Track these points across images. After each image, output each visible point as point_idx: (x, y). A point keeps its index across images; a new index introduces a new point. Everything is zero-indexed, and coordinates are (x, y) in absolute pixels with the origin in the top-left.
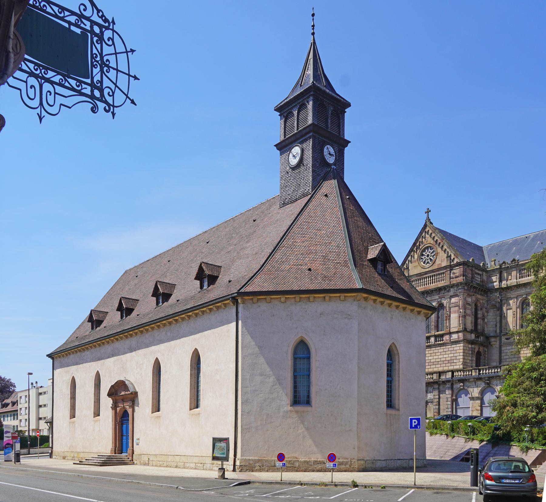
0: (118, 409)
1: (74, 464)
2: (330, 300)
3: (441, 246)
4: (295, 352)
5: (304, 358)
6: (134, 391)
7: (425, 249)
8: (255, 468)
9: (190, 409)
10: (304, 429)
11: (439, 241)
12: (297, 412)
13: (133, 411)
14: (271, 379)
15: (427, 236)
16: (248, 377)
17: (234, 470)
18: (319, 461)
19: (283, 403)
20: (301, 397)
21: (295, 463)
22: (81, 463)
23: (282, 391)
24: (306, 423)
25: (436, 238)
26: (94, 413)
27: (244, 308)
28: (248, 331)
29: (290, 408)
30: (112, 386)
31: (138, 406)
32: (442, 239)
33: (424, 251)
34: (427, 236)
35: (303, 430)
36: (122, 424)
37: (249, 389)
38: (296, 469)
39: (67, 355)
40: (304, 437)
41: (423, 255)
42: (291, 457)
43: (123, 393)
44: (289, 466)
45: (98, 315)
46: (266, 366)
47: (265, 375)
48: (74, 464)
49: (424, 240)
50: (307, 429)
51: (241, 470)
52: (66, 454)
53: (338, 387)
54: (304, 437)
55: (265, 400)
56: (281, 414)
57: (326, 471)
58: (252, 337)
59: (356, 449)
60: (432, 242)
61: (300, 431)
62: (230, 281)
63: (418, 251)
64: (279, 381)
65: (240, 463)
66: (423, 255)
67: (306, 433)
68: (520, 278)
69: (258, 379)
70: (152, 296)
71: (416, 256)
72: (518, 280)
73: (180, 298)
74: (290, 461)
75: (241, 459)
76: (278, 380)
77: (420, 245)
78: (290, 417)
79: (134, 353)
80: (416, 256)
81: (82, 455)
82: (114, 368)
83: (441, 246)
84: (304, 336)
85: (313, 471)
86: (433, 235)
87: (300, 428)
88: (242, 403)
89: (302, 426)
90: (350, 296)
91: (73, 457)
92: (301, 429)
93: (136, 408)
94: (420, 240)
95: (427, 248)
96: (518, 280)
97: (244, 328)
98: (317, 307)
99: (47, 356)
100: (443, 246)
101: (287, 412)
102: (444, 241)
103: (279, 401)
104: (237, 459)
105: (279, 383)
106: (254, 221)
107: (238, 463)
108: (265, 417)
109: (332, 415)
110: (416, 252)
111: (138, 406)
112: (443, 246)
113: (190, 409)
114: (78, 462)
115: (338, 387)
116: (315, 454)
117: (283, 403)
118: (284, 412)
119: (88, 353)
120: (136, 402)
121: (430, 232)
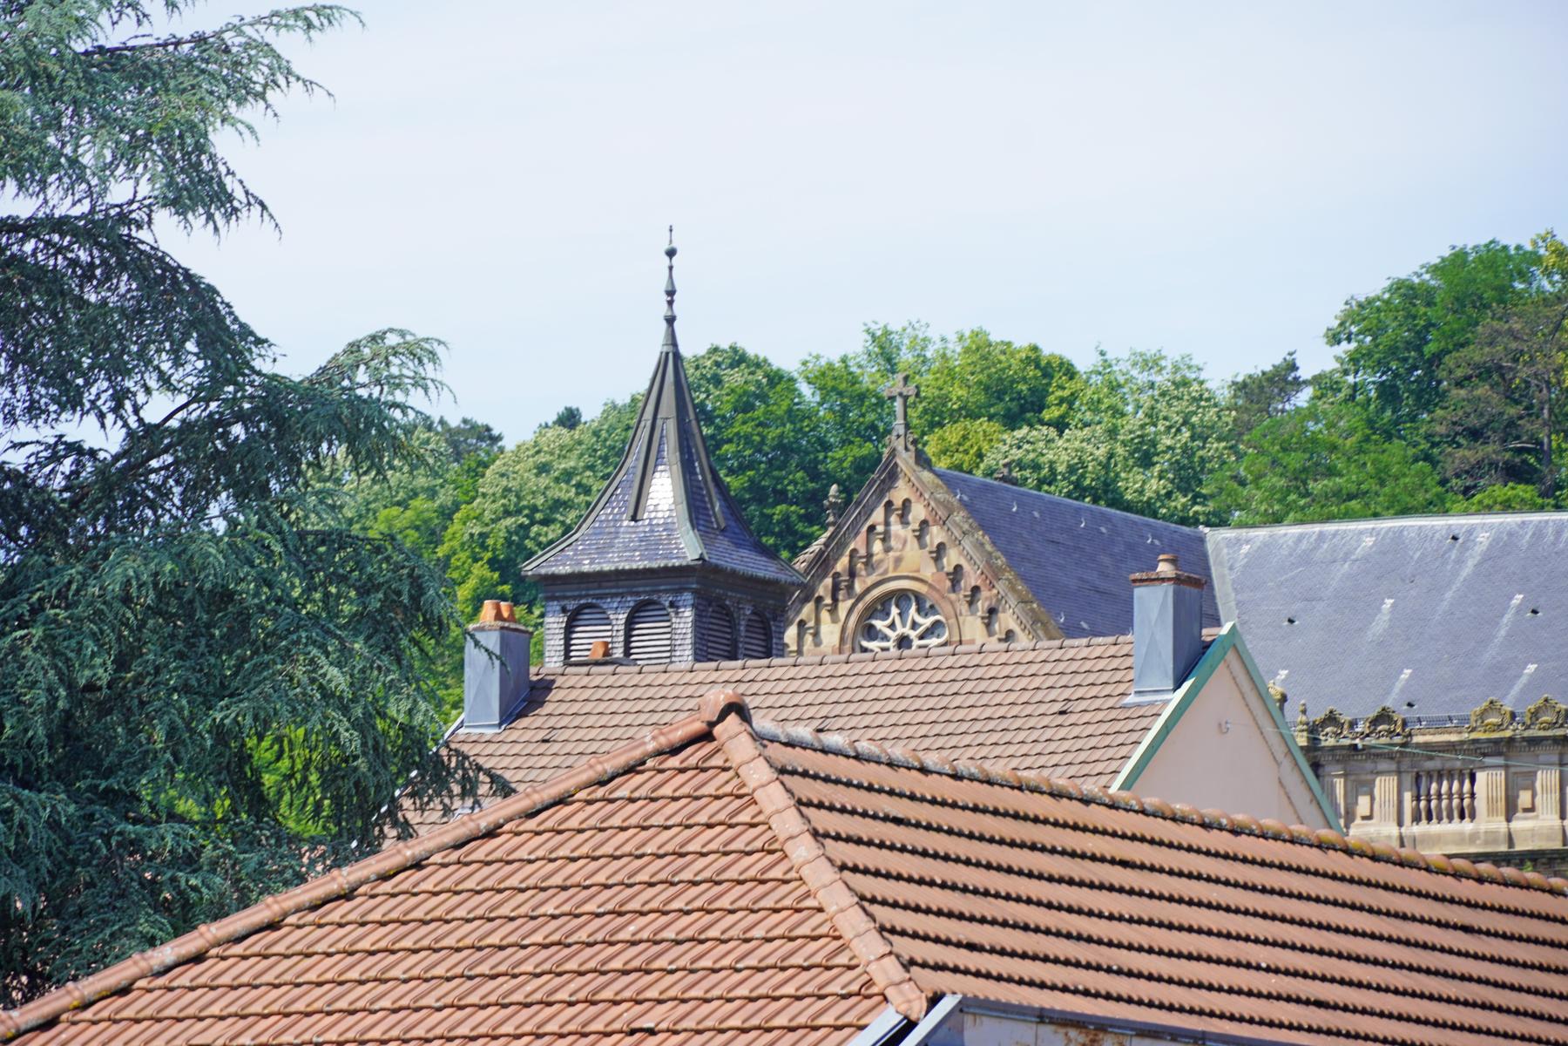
3: (982, 606)
7: (885, 600)
11: (971, 578)
15: (896, 528)
25: (952, 558)
32: (993, 574)
33: (880, 607)
34: (896, 528)
41: (871, 633)
49: (877, 547)
60: (929, 571)
63: (843, 607)
66: (871, 633)
68: (1416, 819)
71: (830, 632)
72: (1411, 829)
77: (852, 574)
80: (830, 632)
83: (982, 606)
86: (936, 535)
94: (858, 543)
95: (901, 597)
96: (1411, 829)
100: (992, 611)
102: (1001, 587)
110: (833, 610)
112: (992, 611)
121: (918, 512)
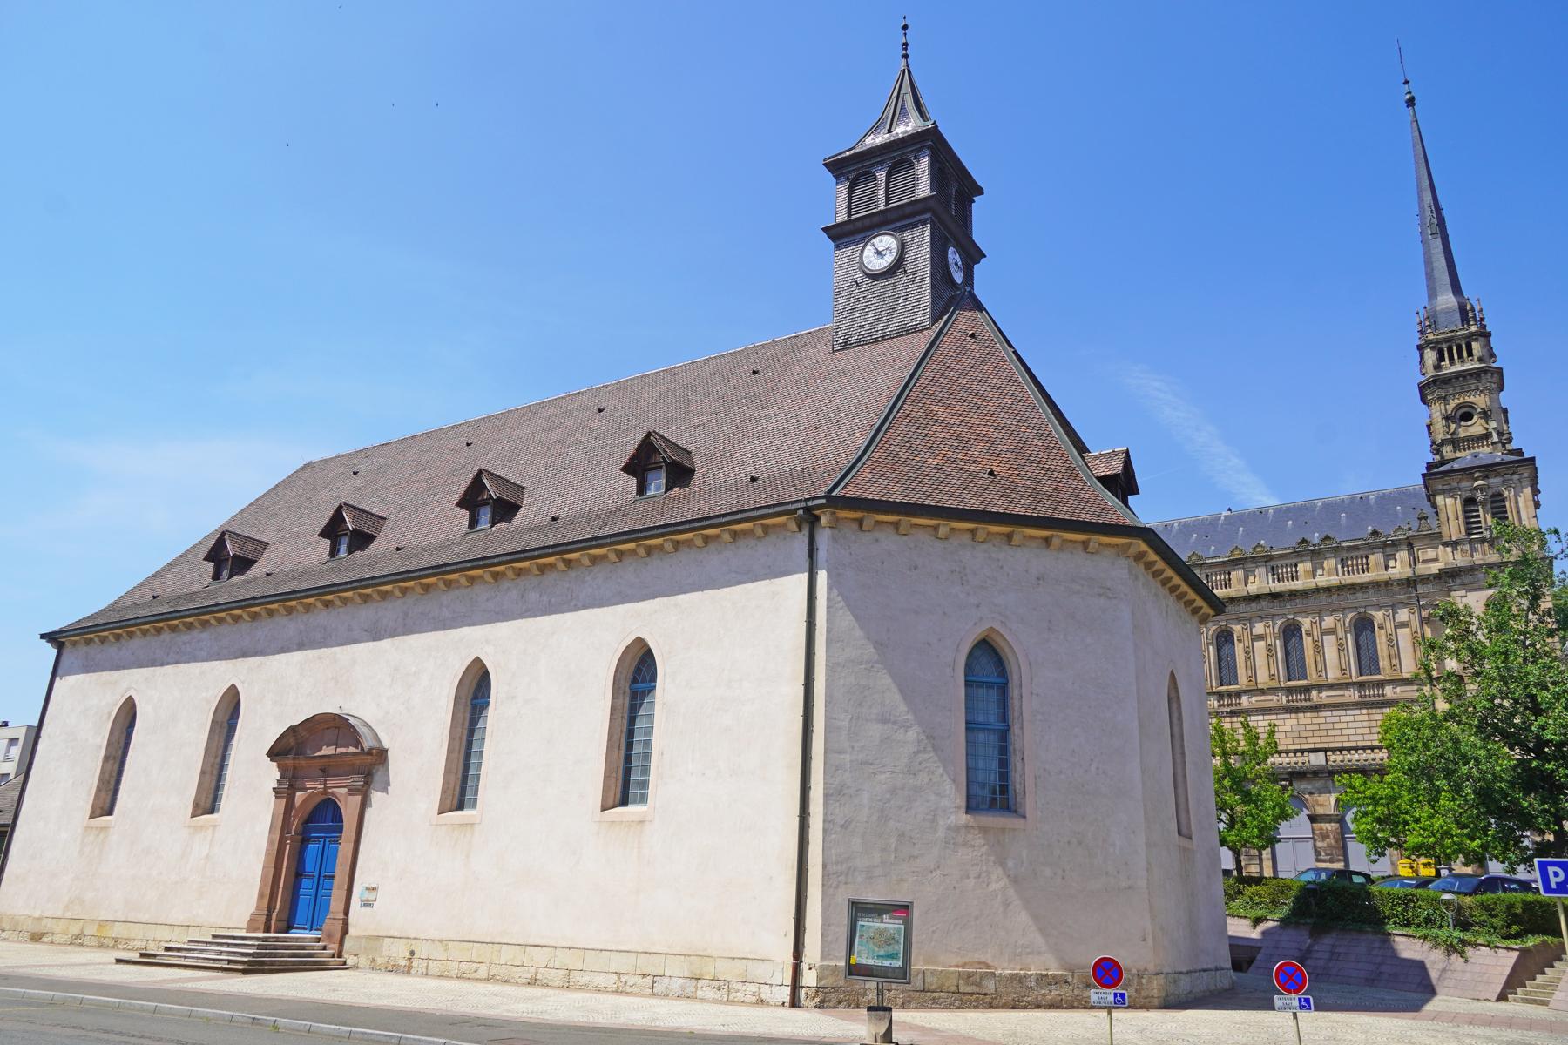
0: (300, 796)
1: (119, 961)
2: (1061, 549)
4: (969, 667)
5: (990, 686)
6: (376, 745)
8: (864, 995)
9: (604, 808)
10: (1005, 881)
12: (984, 830)
13: (365, 804)
14: (912, 734)
16: (846, 724)
17: (795, 1003)
18: (1054, 976)
19: (945, 802)
20: (993, 793)
21: (985, 983)
22: (147, 959)
23: (941, 770)
24: (1010, 864)
26: (196, 805)
27: (834, 539)
28: (845, 599)
29: (964, 818)
30: (292, 730)
31: (385, 790)
35: (1002, 883)
36: (305, 841)
37: (848, 757)
38: (988, 999)
39: (118, 637)
40: (1007, 904)
42: (971, 964)
43: (326, 751)
44: (969, 989)
45: (241, 546)
46: (898, 696)
47: (895, 723)
48: (119, 961)
50: (1015, 880)
51: (822, 1001)
52: (47, 925)
53: (1093, 768)
54: (1007, 904)
55: (893, 791)
56: (941, 834)
57: (1072, 1007)
58: (857, 618)
59: (1150, 942)
61: (994, 886)
62: (753, 479)
64: (932, 738)
65: (819, 979)
67: (1011, 892)
69: (875, 731)
70: (460, 504)
73: (560, 514)
74: (969, 975)
75: (822, 968)
76: (931, 737)
78: (965, 844)
79: (385, 644)
81: (153, 933)
82: (285, 686)
84: (997, 627)
85: (1038, 1007)
87: (994, 877)
88: (826, 796)
89: (1000, 871)
90: (1108, 545)
91: (77, 937)
92: (998, 882)
93: (376, 797)
97: (835, 592)
98: (1027, 559)
99: (43, 636)
101: (957, 829)
103: (933, 797)
104: (804, 966)
105: (935, 749)
106: (755, 373)
107: (809, 979)
108: (893, 842)
109: (1080, 843)
111: (385, 790)
113: (604, 808)
114: (135, 956)
115: (1093, 768)
116: (1039, 953)
117: (945, 802)
118: (949, 828)
119: (205, 635)
120: (378, 777)
